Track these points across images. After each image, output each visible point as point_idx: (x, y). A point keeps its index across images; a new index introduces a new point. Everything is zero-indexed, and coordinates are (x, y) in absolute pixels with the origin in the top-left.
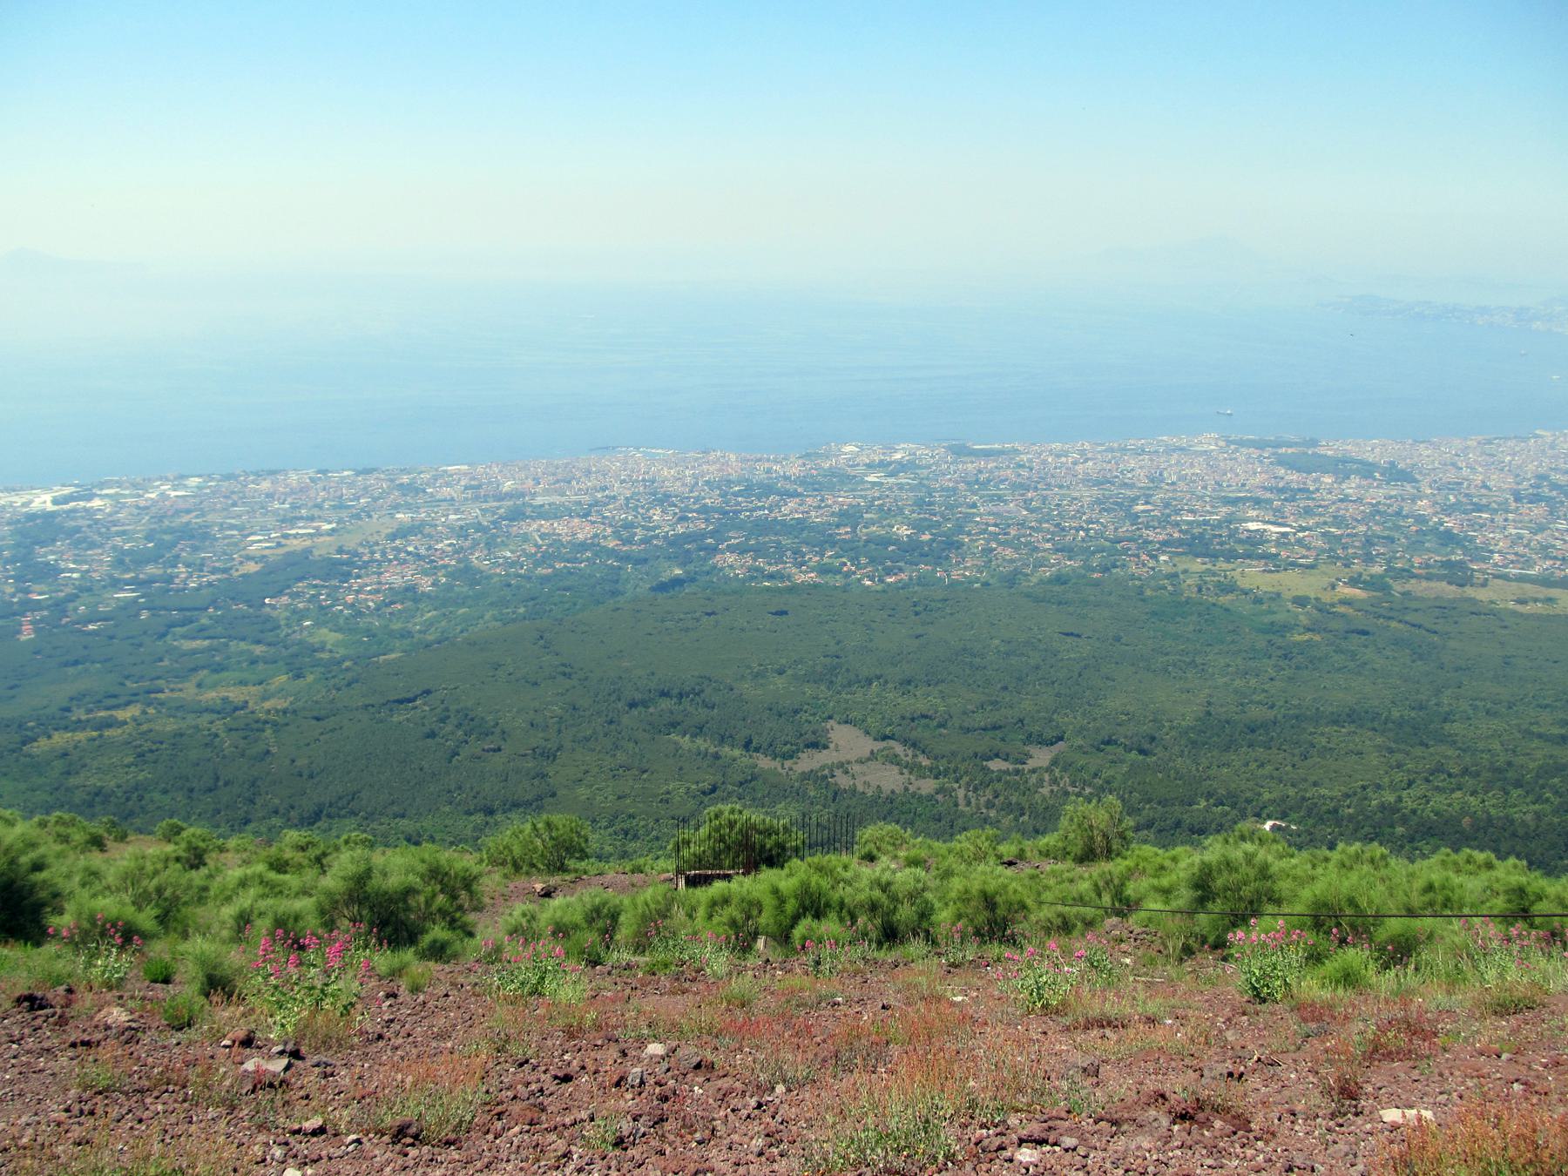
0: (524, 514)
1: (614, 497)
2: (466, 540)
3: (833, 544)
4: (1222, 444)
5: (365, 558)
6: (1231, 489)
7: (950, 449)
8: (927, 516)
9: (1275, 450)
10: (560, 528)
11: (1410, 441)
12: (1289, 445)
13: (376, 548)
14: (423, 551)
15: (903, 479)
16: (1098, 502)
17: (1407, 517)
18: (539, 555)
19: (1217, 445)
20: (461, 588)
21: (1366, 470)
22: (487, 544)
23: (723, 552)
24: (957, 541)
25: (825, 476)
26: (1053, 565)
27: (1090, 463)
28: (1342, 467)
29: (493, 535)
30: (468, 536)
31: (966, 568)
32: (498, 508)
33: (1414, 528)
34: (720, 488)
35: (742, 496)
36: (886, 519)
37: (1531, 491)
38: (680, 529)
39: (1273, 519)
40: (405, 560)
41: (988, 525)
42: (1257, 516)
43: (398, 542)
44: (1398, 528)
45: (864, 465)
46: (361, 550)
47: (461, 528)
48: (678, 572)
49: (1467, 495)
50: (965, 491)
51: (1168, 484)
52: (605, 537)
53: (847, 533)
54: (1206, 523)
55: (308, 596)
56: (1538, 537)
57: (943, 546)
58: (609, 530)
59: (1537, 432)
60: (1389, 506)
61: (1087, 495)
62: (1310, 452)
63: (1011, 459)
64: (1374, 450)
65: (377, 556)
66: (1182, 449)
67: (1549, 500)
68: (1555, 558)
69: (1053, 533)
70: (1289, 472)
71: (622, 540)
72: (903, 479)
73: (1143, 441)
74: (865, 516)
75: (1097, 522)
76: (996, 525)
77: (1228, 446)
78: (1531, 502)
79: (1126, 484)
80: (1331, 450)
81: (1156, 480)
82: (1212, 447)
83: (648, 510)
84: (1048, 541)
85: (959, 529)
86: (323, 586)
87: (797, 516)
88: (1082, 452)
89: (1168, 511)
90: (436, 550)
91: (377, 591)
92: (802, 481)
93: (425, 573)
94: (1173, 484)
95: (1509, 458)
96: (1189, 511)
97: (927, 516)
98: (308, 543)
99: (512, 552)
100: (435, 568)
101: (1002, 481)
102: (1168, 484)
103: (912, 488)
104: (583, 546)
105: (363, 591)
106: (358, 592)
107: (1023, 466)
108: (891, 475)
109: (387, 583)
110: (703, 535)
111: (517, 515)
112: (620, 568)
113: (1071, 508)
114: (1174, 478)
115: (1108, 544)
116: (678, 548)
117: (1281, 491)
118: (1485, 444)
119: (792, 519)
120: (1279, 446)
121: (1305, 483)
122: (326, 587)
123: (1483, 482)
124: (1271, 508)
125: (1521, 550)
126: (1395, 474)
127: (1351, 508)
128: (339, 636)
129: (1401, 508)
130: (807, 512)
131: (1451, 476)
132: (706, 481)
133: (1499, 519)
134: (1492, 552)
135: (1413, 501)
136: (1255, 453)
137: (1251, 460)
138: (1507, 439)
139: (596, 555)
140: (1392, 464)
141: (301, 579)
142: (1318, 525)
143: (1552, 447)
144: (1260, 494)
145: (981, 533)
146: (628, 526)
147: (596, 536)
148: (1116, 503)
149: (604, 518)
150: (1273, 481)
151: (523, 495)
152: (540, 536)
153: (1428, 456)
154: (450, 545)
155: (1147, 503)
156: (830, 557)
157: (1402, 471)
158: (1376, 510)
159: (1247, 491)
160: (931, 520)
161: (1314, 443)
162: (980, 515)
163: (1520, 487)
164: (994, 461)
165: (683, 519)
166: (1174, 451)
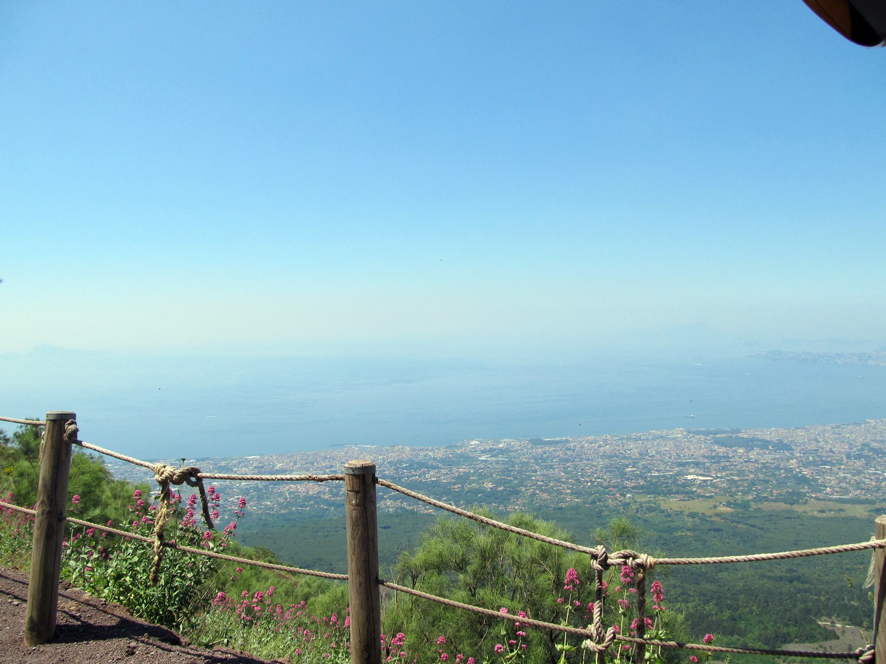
4: (685, 433)
6: (685, 458)
7: (530, 441)
9: (714, 435)
11: (793, 428)
12: (723, 432)
15: (500, 458)
16: (606, 467)
17: (781, 469)
19: (682, 434)
21: (764, 444)
22: (257, 498)
25: (456, 457)
26: (568, 502)
27: (608, 446)
28: (749, 444)
33: (783, 475)
34: (396, 466)
35: (406, 469)
36: (482, 479)
37: (857, 453)
39: (701, 472)
41: (538, 481)
42: (695, 472)
44: (774, 475)
45: (480, 451)
47: (247, 489)
49: (820, 456)
51: (649, 456)
53: (458, 487)
54: (664, 476)
56: (856, 478)
58: (327, 489)
59: (867, 420)
60: (772, 464)
61: (601, 463)
62: (734, 436)
63: (564, 445)
64: (771, 434)
66: (662, 437)
67: (866, 457)
69: (573, 485)
70: (720, 447)
72: (500, 458)
73: (641, 434)
74: (471, 478)
75: (602, 478)
77: (688, 434)
78: (856, 459)
79: (626, 457)
80: (746, 435)
82: (680, 435)
84: (569, 489)
85: (521, 484)
87: (433, 479)
88: (605, 441)
89: (644, 471)
90: (229, 501)
92: (443, 461)
94: (653, 456)
95: (848, 435)
96: (656, 471)
101: (555, 458)
102: (649, 456)
103: (504, 463)
107: (570, 449)
108: (493, 456)
114: (654, 453)
115: (602, 489)
117: (713, 458)
118: (836, 428)
119: (430, 481)
120: (716, 434)
121: (727, 453)
123: (831, 449)
124: (704, 467)
125: (844, 485)
126: (781, 446)
127: (750, 465)
129: (779, 464)
130: (439, 477)
131: (813, 446)
133: (835, 469)
134: (826, 487)
135: (788, 460)
136: (702, 437)
137: (700, 442)
138: (849, 425)
140: (780, 441)
142: (727, 475)
143: (874, 428)
144: (701, 460)
145: (533, 486)
148: (617, 468)
150: (709, 452)
152: (288, 493)
153: (801, 436)
154: (237, 499)
155: (633, 467)
157: (786, 444)
158: (765, 466)
159: (695, 459)
161: (738, 431)
163: (851, 451)
164: (554, 447)
166: (657, 438)
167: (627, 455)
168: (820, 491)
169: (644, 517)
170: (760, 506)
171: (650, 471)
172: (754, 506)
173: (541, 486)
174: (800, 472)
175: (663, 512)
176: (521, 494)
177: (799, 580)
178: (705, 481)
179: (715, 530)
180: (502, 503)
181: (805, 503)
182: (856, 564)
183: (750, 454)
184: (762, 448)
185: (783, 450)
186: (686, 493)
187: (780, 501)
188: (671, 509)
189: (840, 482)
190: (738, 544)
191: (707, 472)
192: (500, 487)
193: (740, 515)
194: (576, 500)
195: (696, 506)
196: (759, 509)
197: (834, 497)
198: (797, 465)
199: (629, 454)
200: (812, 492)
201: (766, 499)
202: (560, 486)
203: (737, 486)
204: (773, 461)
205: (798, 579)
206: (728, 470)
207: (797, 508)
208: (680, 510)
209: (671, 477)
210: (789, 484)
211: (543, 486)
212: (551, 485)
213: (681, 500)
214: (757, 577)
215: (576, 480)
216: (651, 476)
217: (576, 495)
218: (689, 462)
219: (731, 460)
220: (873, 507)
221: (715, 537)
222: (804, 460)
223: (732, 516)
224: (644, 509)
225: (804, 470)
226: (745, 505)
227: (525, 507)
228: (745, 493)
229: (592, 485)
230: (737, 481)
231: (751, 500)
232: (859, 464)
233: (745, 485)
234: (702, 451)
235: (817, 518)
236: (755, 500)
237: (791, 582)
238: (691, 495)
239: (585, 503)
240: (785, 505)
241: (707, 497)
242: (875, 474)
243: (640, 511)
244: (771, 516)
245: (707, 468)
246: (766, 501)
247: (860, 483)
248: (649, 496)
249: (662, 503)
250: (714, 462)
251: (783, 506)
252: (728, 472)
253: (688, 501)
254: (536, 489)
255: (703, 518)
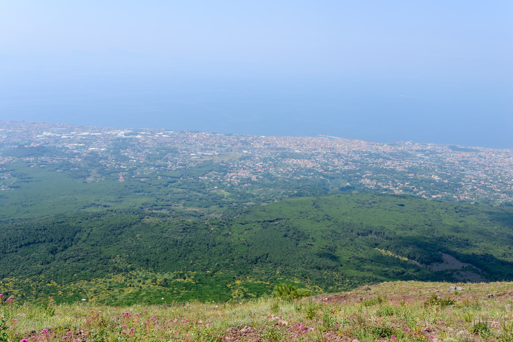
0: (287, 156)
1: (319, 153)
2: (266, 163)
3: (408, 181)
5: (232, 166)
8: (445, 173)
10: (300, 162)
13: (235, 163)
14: (251, 166)
18: (294, 172)
20: (267, 181)
23: (364, 178)
24: (460, 184)
29: (276, 162)
30: (267, 162)
31: (465, 196)
32: (277, 153)
38: (346, 168)
40: (245, 168)
43: (242, 161)
46: (230, 163)
47: (264, 159)
48: (348, 184)
50: (458, 164)
52: (317, 168)
53: (412, 176)
55: (213, 177)
57: (454, 185)
65: (236, 165)
71: (324, 170)
76: (475, 179)
83: (333, 159)
84: (499, 188)
86: (218, 174)
90: (256, 166)
91: (237, 179)
93: (253, 174)
97: (445, 173)
98: (211, 158)
99: (284, 169)
100: (257, 172)
104: (310, 170)
105: (233, 177)
106: (231, 178)
109: (240, 176)
110: (356, 171)
111: (284, 156)
112: (324, 180)
113: (506, 176)
116: (347, 175)
119: (389, 168)
122: (220, 175)
128: (229, 194)
132: (353, 150)
139: (315, 174)
141: (211, 171)
146: (326, 164)
147: (314, 167)
149: (316, 160)
151: (285, 149)
154: (261, 164)
156: (408, 185)
160: (447, 175)
162: (467, 175)
165: (346, 164)
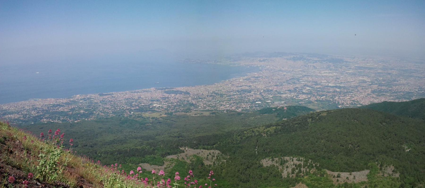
21: (181, 93)
26: (111, 116)
39: (159, 103)
53: (71, 113)
56: (209, 103)
68: (211, 107)
74: (76, 109)
78: (210, 97)
81: (139, 98)
92: (66, 103)
96: (143, 103)
112: (22, 123)
114: (143, 97)
117: (163, 98)
125: (205, 105)
130: (64, 109)
133: (203, 100)
134: (199, 106)
135: (188, 98)
136: (160, 91)
144: (159, 99)
145: (99, 111)
155: (135, 102)
159: (157, 99)
166: (145, 92)
167: (134, 98)
168: (197, 108)
169: (136, 120)
170: (176, 114)
171: (141, 104)
172: (174, 114)
173: (102, 111)
174: (192, 102)
175: (143, 118)
176: (94, 114)
177: (181, 137)
178: (159, 106)
179: (160, 123)
180: (87, 118)
181: (191, 112)
182: (201, 130)
183: (176, 96)
184: (180, 94)
185: (187, 94)
186: (152, 111)
187: (183, 112)
188: (146, 116)
189: (204, 104)
190: (166, 127)
191: (161, 103)
192: (87, 112)
193: (169, 117)
194: (114, 115)
195: (155, 115)
196: (176, 115)
197: (201, 110)
198: (191, 99)
199: (134, 98)
200: (194, 108)
201: (179, 111)
202: (108, 110)
203: (170, 108)
204: (183, 98)
205: (181, 136)
206: (168, 102)
207: (188, 114)
208: (149, 116)
209: (148, 106)
210: (187, 106)
211: (102, 111)
212: (105, 110)
213: (150, 113)
214: (168, 137)
215: (114, 108)
216: (141, 105)
217: (114, 114)
218: (155, 100)
219: (169, 98)
220: (211, 112)
221: (159, 125)
222: (193, 98)
223: (166, 118)
224: (136, 117)
225: (193, 101)
226: (171, 114)
227: (95, 118)
228: (172, 110)
229: (120, 109)
230: (170, 106)
231: (173, 112)
232: (211, 98)
233: (173, 107)
234: (160, 96)
235: (193, 117)
236: (175, 112)
237: (179, 137)
238: (154, 111)
239: (116, 116)
240: (184, 113)
241: (159, 112)
242: (215, 101)
243: (135, 117)
244: (178, 117)
245: (161, 102)
246: (178, 112)
247: (210, 105)
248: (139, 112)
249: (143, 114)
250: (164, 100)
251: (183, 113)
252: (168, 103)
253: (152, 114)
254: (100, 112)
255: (156, 119)
